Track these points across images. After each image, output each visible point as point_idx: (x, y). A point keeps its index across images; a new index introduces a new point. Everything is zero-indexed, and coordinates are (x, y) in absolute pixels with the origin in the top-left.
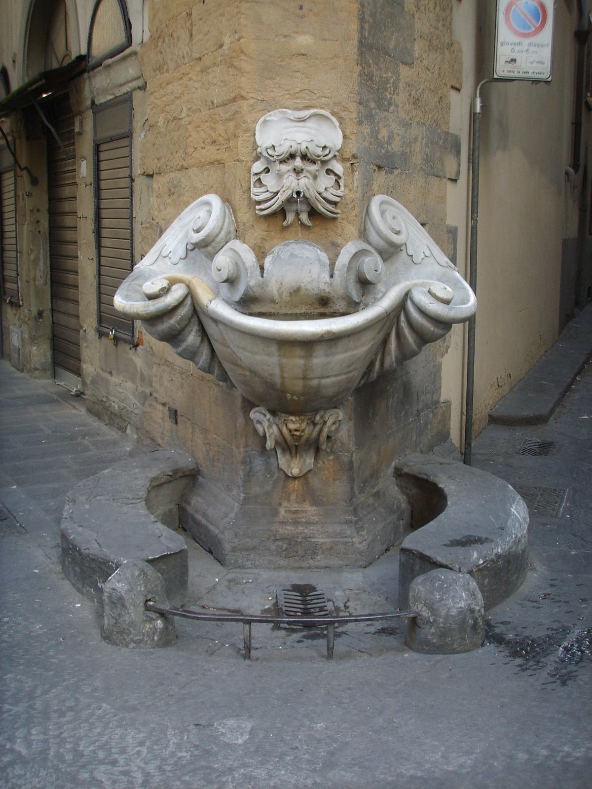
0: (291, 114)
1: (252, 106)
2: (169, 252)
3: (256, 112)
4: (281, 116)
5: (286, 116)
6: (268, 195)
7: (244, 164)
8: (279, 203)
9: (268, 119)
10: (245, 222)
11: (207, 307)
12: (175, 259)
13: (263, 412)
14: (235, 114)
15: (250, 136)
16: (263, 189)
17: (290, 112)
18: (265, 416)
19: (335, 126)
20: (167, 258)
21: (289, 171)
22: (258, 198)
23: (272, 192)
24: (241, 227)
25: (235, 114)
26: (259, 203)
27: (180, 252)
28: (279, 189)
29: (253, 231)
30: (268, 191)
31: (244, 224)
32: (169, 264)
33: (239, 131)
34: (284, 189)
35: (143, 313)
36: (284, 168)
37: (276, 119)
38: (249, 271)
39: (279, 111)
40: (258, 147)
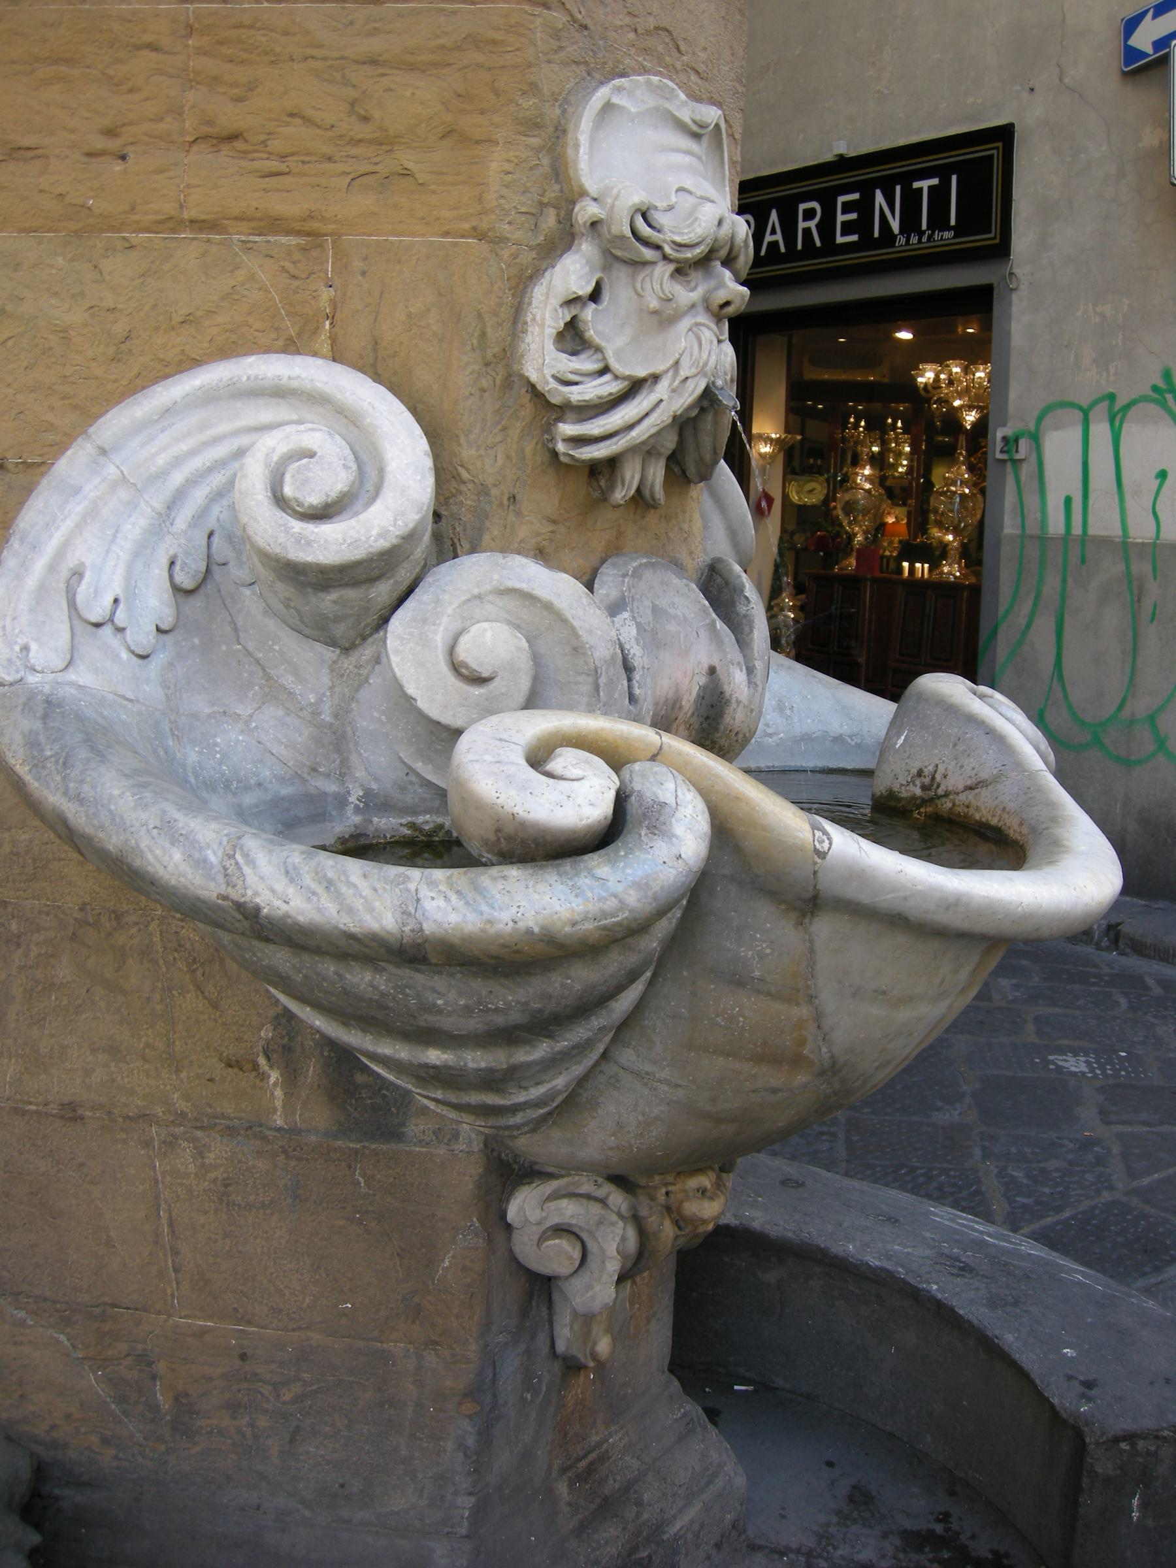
0: (684, 103)
1: (556, 34)
2: (108, 600)
3: (564, 64)
4: (651, 101)
5: (668, 105)
6: (606, 387)
7: (506, 254)
8: (660, 418)
9: (615, 100)
10: (490, 481)
11: (822, 855)
12: (142, 635)
13: (587, 1188)
14: (458, 48)
15: (538, 150)
16: (586, 363)
17: (683, 96)
18: (603, 1201)
19: (724, 177)
20: (107, 630)
21: (693, 306)
22: (576, 394)
23: (625, 378)
24: (468, 499)
25: (458, 48)
26: (565, 410)
27: (154, 602)
28: (658, 368)
29: (512, 518)
30: (605, 370)
31: (484, 491)
32: (124, 655)
33: (496, 119)
34: (683, 373)
35: (589, 926)
36: (686, 294)
37: (633, 110)
38: (603, 681)
39: (649, 83)
40: (583, 193)
